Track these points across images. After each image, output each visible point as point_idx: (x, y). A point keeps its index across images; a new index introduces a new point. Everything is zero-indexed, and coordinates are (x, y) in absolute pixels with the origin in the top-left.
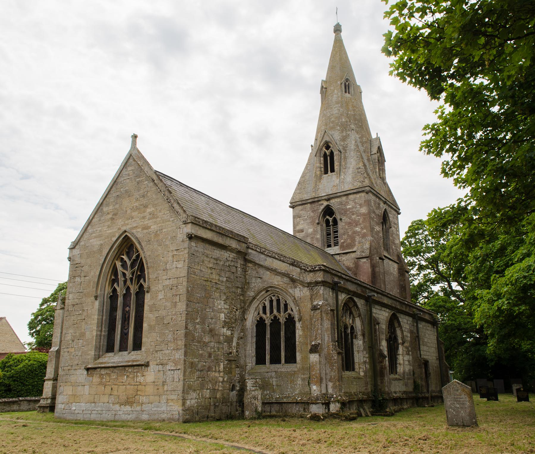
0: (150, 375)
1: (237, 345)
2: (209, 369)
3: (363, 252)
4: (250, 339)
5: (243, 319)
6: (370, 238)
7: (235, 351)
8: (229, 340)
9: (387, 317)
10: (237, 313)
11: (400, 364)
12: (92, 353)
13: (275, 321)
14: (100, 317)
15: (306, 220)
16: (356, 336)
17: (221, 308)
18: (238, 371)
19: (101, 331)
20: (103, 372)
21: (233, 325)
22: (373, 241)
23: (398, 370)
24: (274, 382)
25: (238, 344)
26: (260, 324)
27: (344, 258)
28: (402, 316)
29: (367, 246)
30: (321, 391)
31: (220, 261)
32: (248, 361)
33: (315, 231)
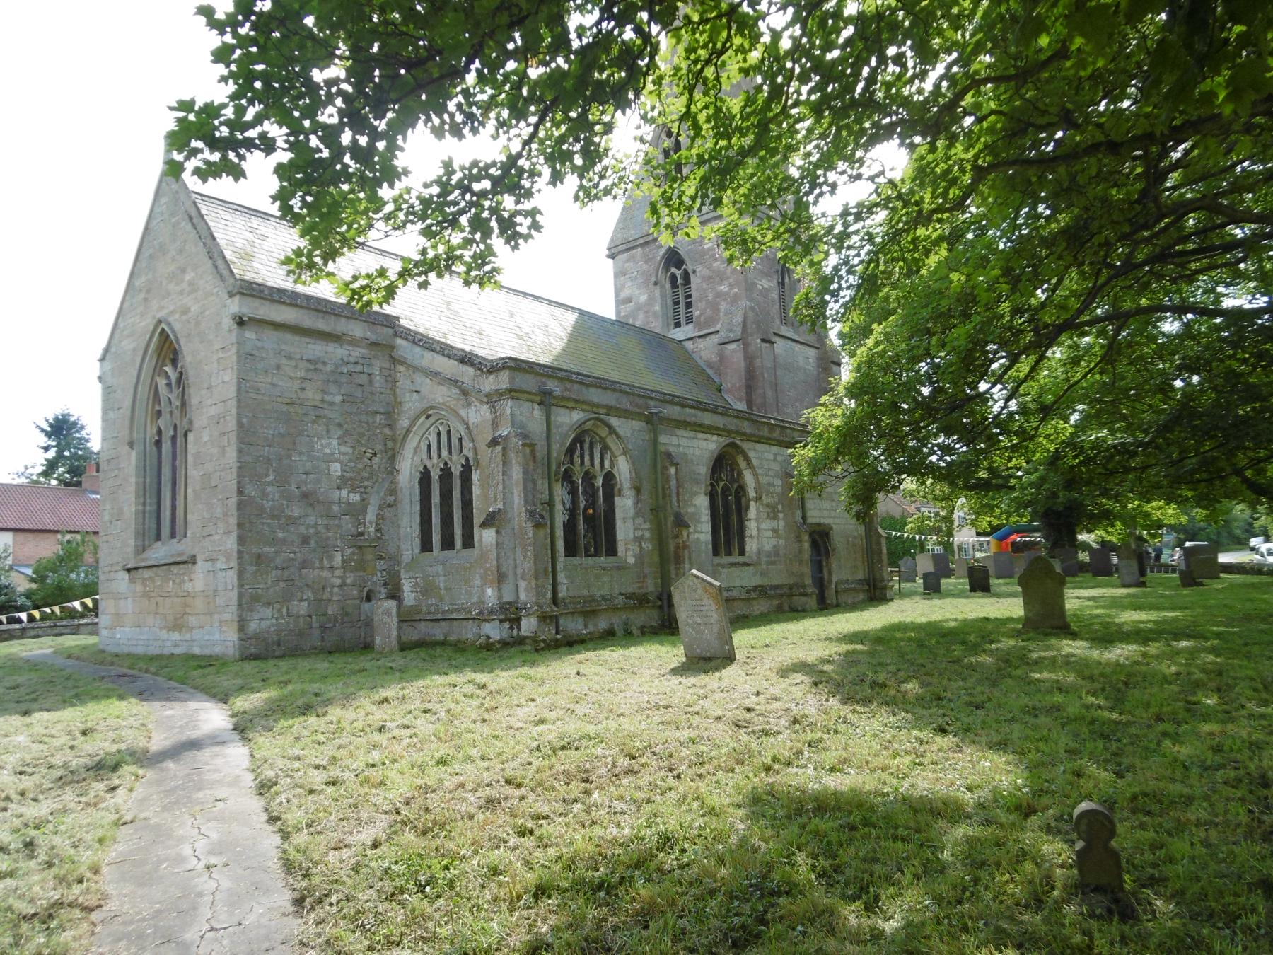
0: (198, 579)
1: (378, 519)
2: (304, 565)
3: (731, 331)
4: (408, 507)
5: (392, 471)
6: (744, 303)
7: (372, 530)
8: (357, 512)
9: (712, 452)
10: (376, 460)
11: (751, 537)
12: (132, 542)
13: (446, 473)
14: (141, 480)
15: (636, 278)
16: (620, 490)
17: (331, 454)
18: (381, 565)
19: (144, 504)
20: (146, 574)
21: (366, 483)
22: (752, 308)
23: (747, 548)
24: (441, 582)
25: (380, 518)
26: (425, 478)
27: (702, 344)
28: (751, 445)
29: (739, 318)
30: (500, 598)
31: (324, 363)
32: (403, 547)
33: (651, 300)
